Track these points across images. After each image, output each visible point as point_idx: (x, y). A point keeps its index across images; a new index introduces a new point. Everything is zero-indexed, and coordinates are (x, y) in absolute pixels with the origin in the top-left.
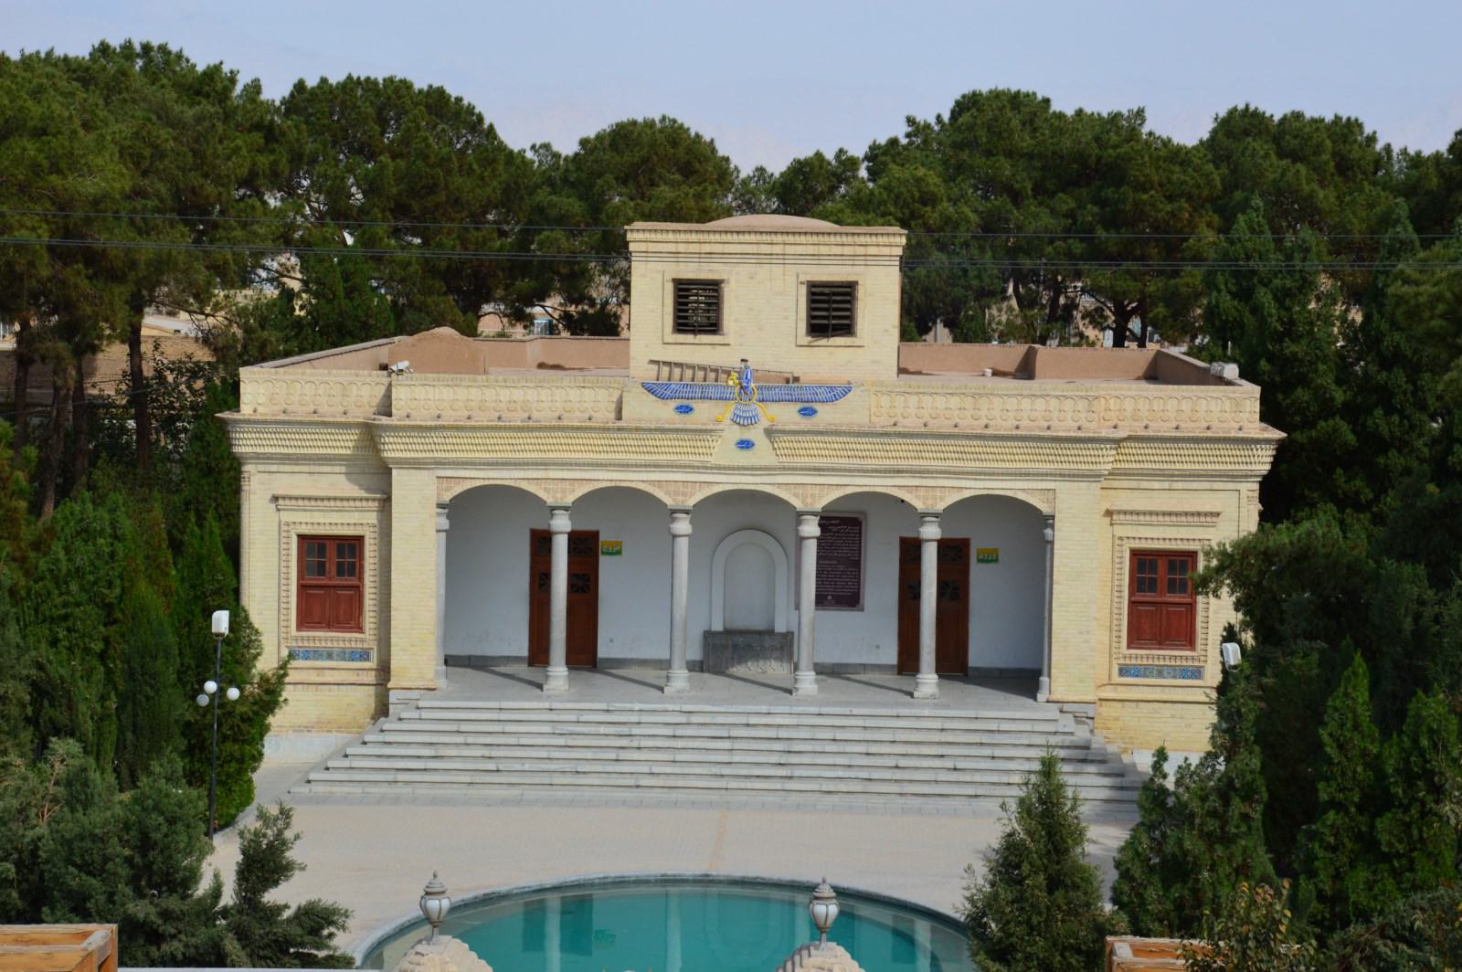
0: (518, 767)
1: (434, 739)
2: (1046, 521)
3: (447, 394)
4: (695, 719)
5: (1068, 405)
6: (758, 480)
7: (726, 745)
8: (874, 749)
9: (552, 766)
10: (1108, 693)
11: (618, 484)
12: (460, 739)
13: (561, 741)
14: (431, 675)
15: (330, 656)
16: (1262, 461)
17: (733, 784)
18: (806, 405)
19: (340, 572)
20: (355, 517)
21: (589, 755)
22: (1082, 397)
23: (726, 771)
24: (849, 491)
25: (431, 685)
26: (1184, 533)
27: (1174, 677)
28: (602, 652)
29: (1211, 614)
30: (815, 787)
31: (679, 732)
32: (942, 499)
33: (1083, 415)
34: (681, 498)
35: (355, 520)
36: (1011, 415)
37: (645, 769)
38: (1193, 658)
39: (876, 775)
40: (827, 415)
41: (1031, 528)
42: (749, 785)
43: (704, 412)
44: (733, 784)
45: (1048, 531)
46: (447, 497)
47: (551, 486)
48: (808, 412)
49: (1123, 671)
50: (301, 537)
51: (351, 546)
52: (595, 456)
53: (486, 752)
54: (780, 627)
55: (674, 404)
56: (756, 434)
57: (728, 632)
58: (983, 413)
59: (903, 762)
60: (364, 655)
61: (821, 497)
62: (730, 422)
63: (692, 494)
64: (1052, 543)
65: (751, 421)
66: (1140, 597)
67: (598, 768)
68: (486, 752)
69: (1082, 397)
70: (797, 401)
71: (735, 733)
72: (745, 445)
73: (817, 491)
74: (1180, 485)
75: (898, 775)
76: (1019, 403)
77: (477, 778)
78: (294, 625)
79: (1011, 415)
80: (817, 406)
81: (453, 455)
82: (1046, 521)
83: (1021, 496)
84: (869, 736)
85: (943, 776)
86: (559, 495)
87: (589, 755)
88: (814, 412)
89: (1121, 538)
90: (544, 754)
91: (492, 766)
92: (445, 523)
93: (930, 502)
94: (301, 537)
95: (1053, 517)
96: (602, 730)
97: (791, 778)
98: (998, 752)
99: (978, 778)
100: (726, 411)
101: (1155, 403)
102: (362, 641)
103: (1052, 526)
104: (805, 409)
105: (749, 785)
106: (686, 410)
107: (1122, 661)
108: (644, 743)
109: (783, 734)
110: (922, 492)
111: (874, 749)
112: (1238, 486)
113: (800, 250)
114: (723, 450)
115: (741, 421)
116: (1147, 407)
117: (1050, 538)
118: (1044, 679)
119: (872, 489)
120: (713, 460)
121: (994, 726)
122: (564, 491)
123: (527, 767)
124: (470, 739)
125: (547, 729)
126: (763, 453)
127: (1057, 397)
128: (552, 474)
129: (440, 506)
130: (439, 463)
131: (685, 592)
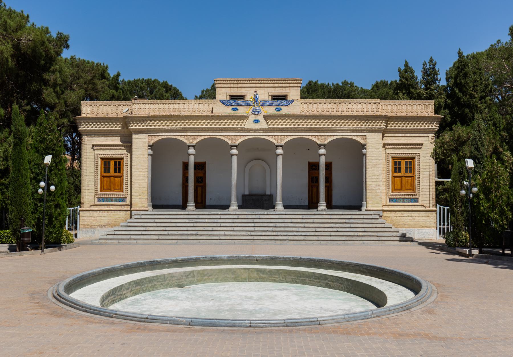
0: (176, 233)
2: (364, 146)
3: (152, 106)
4: (240, 217)
5: (370, 106)
7: (253, 225)
8: (307, 225)
10: (386, 208)
12: (155, 224)
13: (192, 224)
14: (146, 206)
15: (112, 201)
16: (435, 126)
17: (256, 238)
19: (115, 172)
20: (120, 152)
21: (202, 229)
22: (374, 103)
23: (253, 233)
25: (146, 209)
27: (408, 202)
28: (208, 203)
29: (420, 179)
31: (235, 221)
32: (327, 139)
33: (375, 109)
35: (121, 152)
36: (350, 110)
37: (223, 233)
38: (415, 195)
39: (308, 234)
40: (285, 110)
41: (357, 151)
42: (261, 238)
43: (242, 111)
44: (256, 238)
45: (365, 150)
46: (152, 142)
47: (188, 137)
49: (391, 200)
50: (102, 159)
51: (118, 162)
53: (164, 228)
54: (268, 193)
55: (231, 108)
56: (260, 118)
57: (250, 195)
58: (340, 109)
59: (318, 229)
60: (124, 200)
61: (284, 140)
62: (250, 113)
63: (238, 140)
64: (365, 154)
66: (396, 174)
67: (205, 233)
68: (164, 228)
69: (374, 103)
71: (255, 221)
72: (256, 121)
73: (282, 137)
75: (316, 234)
76: (352, 106)
77: (161, 237)
78: (99, 189)
79: (350, 110)
82: (364, 146)
83: (354, 138)
84: (304, 221)
85: (333, 234)
87: (202, 229)
88: (281, 109)
89: (388, 154)
90: (185, 229)
91: (166, 233)
92: (151, 152)
93: (322, 141)
94: (102, 159)
95: (366, 145)
96: (207, 221)
97: (277, 235)
98: (352, 225)
99: (346, 234)
101: (399, 106)
102: (123, 195)
103: (366, 149)
104: (277, 108)
105: (261, 238)
106: (236, 109)
107: (390, 197)
108: (222, 225)
109: (273, 221)
110: (319, 137)
111: (307, 225)
112: (428, 135)
113: (269, 85)
114: (249, 124)
115: (256, 113)
116: (396, 108)
117: (365, 153)
118: (364, 203)
120: (245, 127)
121: (349, 217)
122: (193, 140)
123: (179, 233)
124: (159, 224)
125: (187, 220)
126: (263, 125)
127: (366, 103)
129: (149, 146)
131: (236, 175)
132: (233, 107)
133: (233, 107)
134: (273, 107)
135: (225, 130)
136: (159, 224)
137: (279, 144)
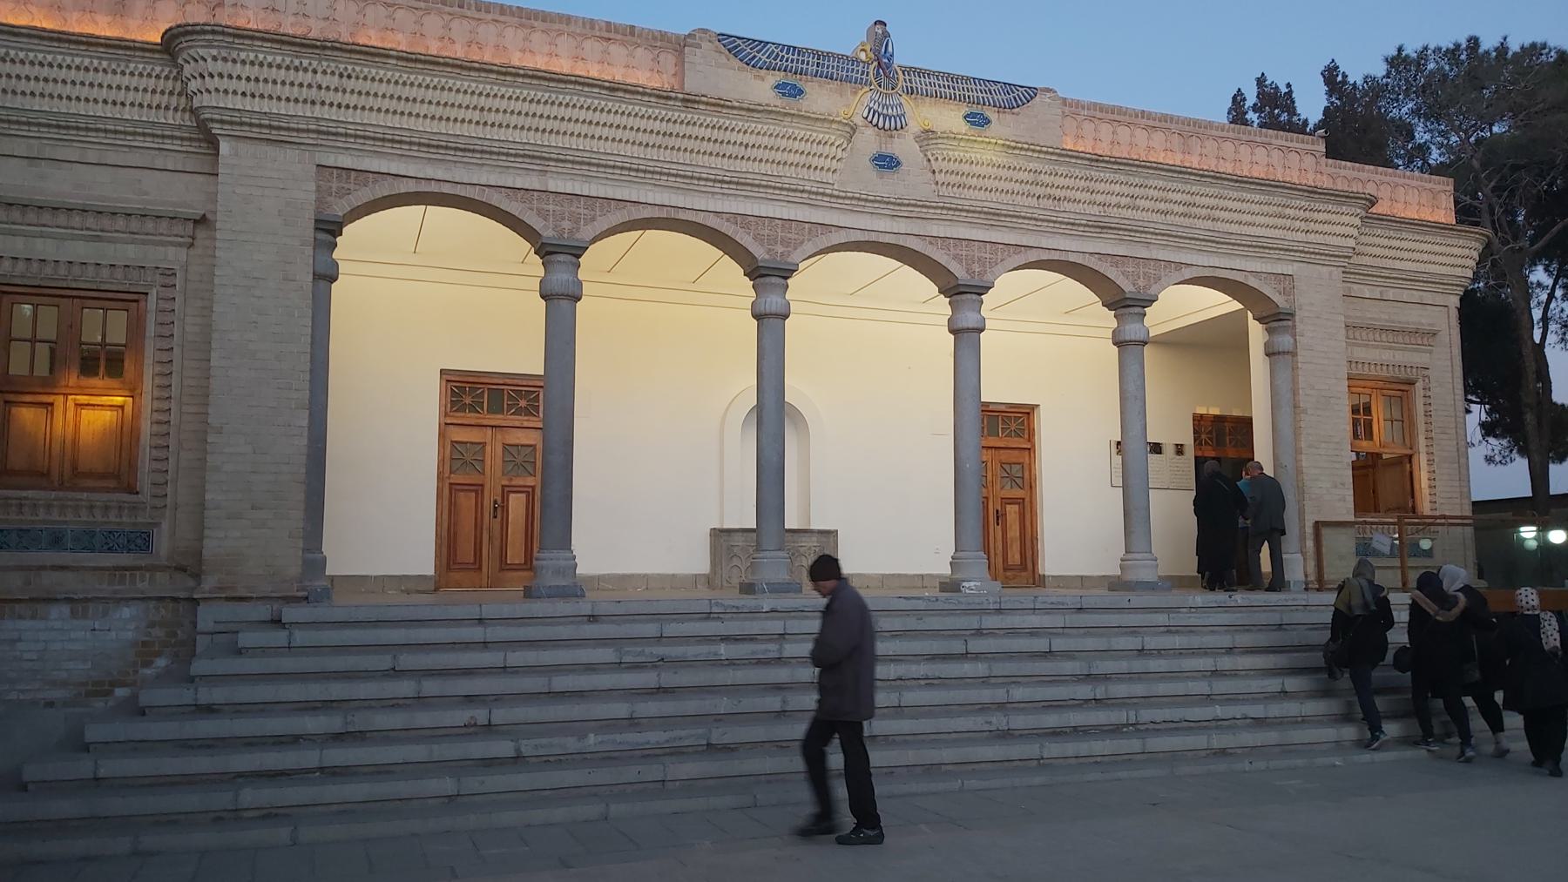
0: (572, 744)
1: (337, 690)
6: (902, 226)
9: (655, 737)
15: (56, 541)
18: (976, 109)
26: (1400, 357)
30: (1198, 741)
34: (780, 249)
43: (820, 98)
70: (963, 99)
72: (887, 162)
74: (1391, 294)
80: (990, 113)
81: (358, 117)
86: (566, 224)
88: (989, 122)
96: (724, 650)
100: (857, 104)
102: (134, 508)
106: (796, 92)
124: (431, 687)
128: (555, 184)
130: (326, 134)
133: (778, 77)
134: (953, 105)
135: (739, 184)
136: (431, 687)
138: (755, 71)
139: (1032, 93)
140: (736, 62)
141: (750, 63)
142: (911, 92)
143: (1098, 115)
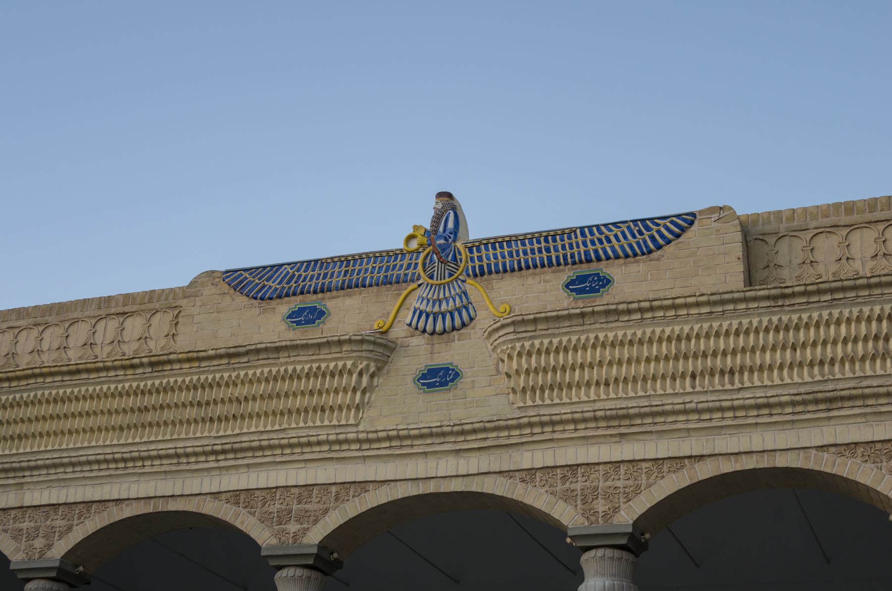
11: (162, 507)
18: (584, 269)
24: (705, 471)
43: (349, 315)
48: (588, 285)
52: (112, 439)
55: (284, 308)
65: (459, 321)
72: (439, 378)
80: (614, 270)
88: (605, 282)
104: (582, 279)
119: (765, 463)
128: (32, 497)
132: (295, 303)
133: (295, 303)
134: (548, 274)
137: (600, 527)
138: (264, 304)
139: (690, 219)
140: (242, 300)
141: (263, 297)
142: (479, 273)
143: (844, 219)
